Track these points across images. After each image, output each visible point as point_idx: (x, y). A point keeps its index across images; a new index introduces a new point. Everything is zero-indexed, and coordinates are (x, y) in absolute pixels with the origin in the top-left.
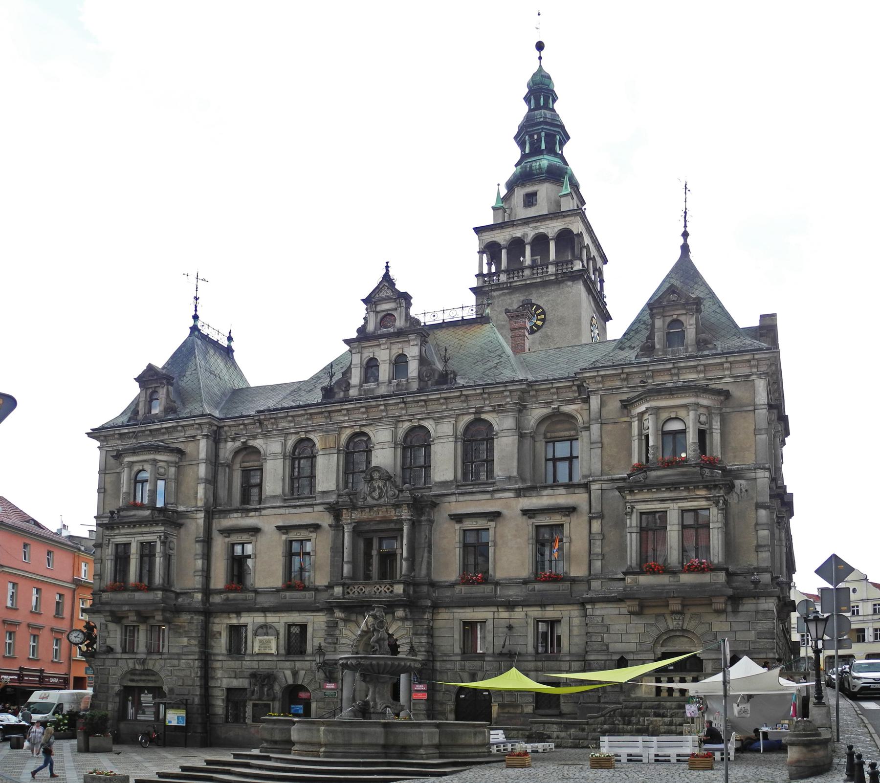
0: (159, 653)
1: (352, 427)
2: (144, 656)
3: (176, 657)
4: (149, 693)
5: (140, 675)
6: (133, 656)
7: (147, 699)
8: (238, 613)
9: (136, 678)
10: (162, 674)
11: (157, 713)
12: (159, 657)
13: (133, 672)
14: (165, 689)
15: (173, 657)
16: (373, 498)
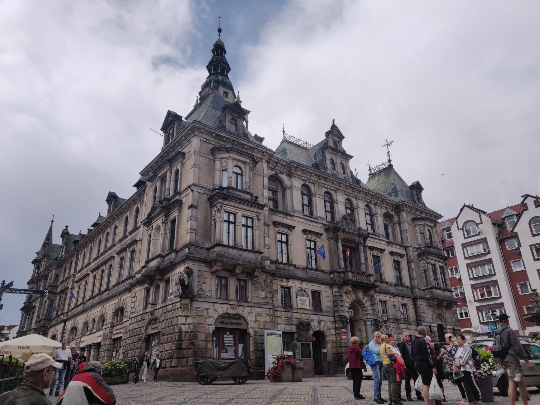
0: (246, 301)
1: (327, 188)
2: (235, 303)
3: (258, 306)
4: (230, 334)
5: (229, 318)
6: (226, 302)
7: (228, 339)
8: (288, 278)
9: (226, 321)
10: (249, 319)
11: (236, 352)
12: (246, 304)
13: (223, 316)
14: (251, 331)
15: (256, 305)
16: (349, 229)
